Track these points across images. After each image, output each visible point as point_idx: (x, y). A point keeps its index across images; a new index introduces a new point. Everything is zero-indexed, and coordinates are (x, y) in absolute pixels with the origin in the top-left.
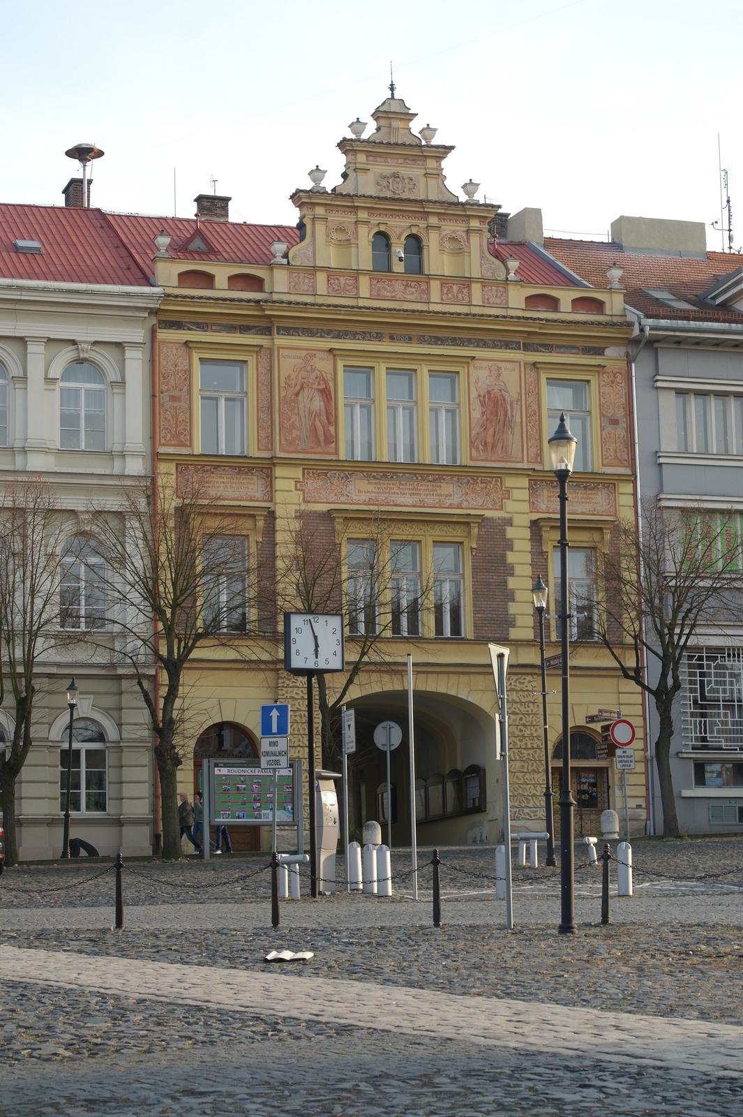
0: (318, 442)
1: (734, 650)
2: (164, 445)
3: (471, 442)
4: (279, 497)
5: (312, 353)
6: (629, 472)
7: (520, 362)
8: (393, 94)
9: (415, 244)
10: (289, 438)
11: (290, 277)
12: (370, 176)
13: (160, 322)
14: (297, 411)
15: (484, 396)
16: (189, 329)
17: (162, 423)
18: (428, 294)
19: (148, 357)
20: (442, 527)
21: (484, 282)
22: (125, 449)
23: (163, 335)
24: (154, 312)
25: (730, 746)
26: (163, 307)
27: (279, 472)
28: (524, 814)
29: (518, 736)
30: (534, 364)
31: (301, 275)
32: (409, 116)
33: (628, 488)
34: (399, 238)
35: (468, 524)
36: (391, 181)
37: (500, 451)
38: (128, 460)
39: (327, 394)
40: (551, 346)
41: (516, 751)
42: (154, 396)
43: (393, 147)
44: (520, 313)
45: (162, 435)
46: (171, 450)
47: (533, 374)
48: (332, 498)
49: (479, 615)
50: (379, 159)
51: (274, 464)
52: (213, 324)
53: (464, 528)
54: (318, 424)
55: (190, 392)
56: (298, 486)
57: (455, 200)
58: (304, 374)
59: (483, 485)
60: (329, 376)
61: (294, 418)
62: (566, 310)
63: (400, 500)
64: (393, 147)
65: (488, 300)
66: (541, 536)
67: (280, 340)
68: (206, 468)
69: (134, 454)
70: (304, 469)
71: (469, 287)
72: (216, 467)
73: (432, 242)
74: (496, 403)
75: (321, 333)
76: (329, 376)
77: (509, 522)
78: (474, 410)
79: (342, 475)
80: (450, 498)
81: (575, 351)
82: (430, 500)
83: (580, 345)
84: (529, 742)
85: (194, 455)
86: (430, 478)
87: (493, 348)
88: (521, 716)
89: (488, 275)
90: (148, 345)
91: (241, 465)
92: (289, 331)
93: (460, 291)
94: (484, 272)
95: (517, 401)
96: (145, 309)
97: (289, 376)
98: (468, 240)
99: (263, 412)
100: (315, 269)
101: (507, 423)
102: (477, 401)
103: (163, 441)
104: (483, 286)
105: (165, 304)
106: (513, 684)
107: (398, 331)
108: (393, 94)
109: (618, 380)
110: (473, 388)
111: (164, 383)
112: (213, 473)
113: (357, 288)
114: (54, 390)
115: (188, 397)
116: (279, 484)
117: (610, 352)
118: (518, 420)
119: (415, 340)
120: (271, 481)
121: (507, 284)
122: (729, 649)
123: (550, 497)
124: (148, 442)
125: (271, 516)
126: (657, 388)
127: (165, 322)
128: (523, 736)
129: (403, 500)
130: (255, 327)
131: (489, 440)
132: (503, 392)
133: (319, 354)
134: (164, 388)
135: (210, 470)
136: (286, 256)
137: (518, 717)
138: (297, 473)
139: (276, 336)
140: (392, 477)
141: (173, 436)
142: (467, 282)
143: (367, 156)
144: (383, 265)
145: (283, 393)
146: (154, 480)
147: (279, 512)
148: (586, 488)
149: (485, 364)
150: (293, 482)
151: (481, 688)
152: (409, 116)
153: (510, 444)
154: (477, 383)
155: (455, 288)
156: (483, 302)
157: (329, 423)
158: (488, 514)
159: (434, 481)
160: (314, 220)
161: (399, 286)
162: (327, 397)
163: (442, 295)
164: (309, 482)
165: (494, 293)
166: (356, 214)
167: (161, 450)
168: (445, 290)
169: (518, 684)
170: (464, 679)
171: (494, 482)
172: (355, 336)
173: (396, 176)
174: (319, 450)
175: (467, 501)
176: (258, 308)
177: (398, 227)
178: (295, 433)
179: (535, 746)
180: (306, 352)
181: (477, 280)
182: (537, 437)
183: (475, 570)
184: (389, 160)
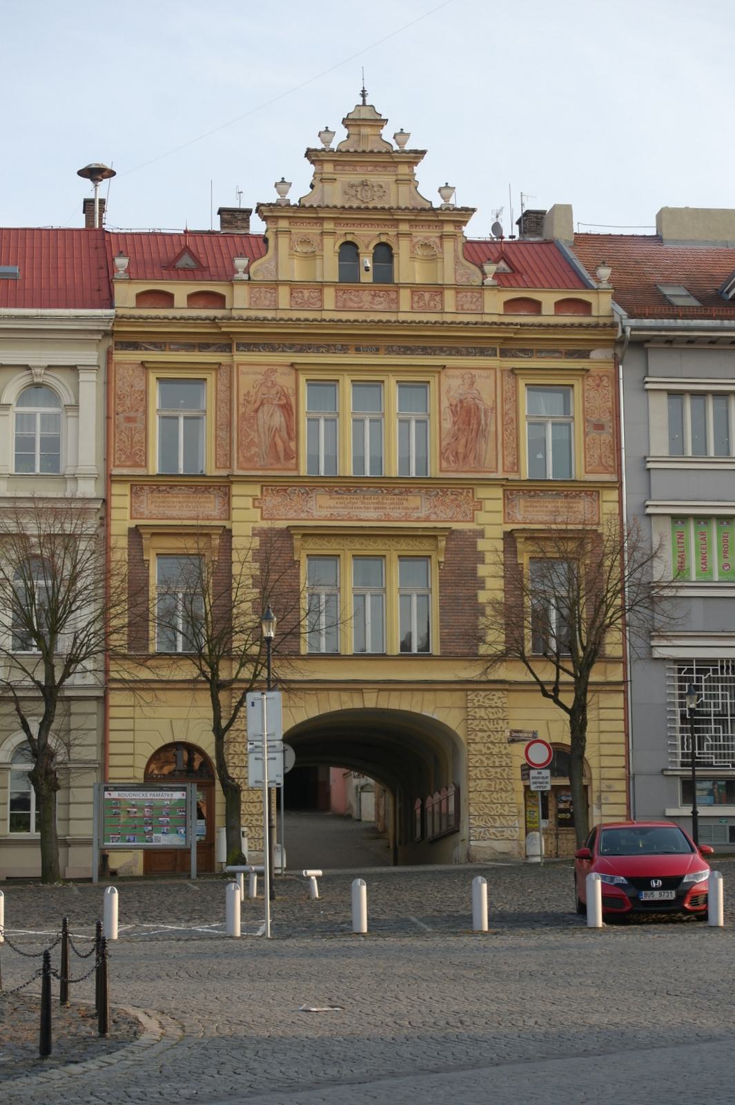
0: (278, 458)
2: (118, 466)
3: (441, 453)
4: (235, 515)
5: (272, 368)
6: (614, 478)
7: (495, 369)
8: (364, 101)
9: (384, 253)
10: (248, 455)
11: (251, 292)
12: (338, 185)
13: (116, 343)
14: (255, 428)
15: (456, 406)
16: (146, 349)
17: (117, 445)
18: (398, 303)
19: (102, 378)
20: (408, 541)
21: (458, 288)
22: (77, 472)
23: (119, 356)
24: (107, 334)
25: (720, 762)
26: (115, 329)
27: (235, 489)
28: (490, 834)
29: (486, 754)
30: (512, 370)
31: (263, 290)
32: (380, 122)
33: (614, 495)
34: (367, 247)
35: (435, 537)
36: (359, 189)
37: (472, 462)
38: (81, 482)
39: (288, 409)
40: (532, 351)
41: (483, 769)
42: (108, 418)
43: (365, 153)
44: (496, 319)
45: (116, 456)
46: (125, 471)
47: (511, 380)
48: (292, 514)
49: (447, 631)
50: (347, 168)
51: (232, 482)
52: (171, 343)
53: (432, 541)
54: (278, 440)
56: (257, 504)
57: (428, 206)
58: (264, 389)
59: (453, 497)
60: (290, 391)
61: (253, 435)
62: (549, 314)
63: (364, 514)
64: (365, 153)
65: (462, 306)
66: (516, 547)
67: (240, 357)
68: (161, 488)
69: (86, 477)
70: (262, 486)
71: (442, 293)
72: (172, 487)
73: (402, 250)
74: (468, 412)
75: (283, 348)
76: (290, 391)
77: (481, 534)
78: (445, 420)
79: (302, 491)
80: (418, 511)
81: (557, 355)
82: (395, 514)
83: (563, 348)
84: (497, 760)
85: (148, 476)
86: (397, 491)
87: (467, 355)
88: (490, 733)
89: (463, 281)
90: (103, 366)
91: (198, 484)
92: (249, 347)
93: (432, 298)
94: (458, 278)
96: (98, 331)
97: (248, 393)
98: (442, 246)
100: (277, 284)
101: (480, 432)
102: (448, 411)
103: (117, 463)
104: (457, 293)
105: (118, 326)
106: (481, 700)
107: (365, 343)
108: (364, 101)
109: (605, 383)
110: (444, 398)
111: (119, 404)
112: (168, 493)
113: (321, 300)
114: (7, 415)
115: (144, 417)
116: (235, 502)
117: (596, 354)
118: (492, 428)
120: (229, 499)
121: (483, 289)
123: (527, 507)
124: (102, 465)
125: (227, 534)
127: (122, 343)
128: (491, 753)
129: (367, 514)
130: (214, 344)
131: (461, 450)
132: (477, 401)
133: (280, 369)
134: (120, 409)
135: (165, 490)
136: (247, 271)
137: (485, 735)
138: (256, 490)
139: (235, 352)
140: (355, 491)
141: (128, 457)
142: (439, 289)
143: (335, 166)
144: (349, 275)
145: (242, 410)
146: (105, 502)
147: (236, 529)
148: (566, 496)
149: (457, 372)
150: (250, 500)
151: (447, 705)
152: (380, 122)
153: (484, 453)
154: (448, 392)
155: (427, 296)
156: (457, 309)
157: (290, 438)
158: (455, 526)
159: (401, 494)
160: (277, 233)
161: (366, 296)
162: (288, 413)
163: (412, 303)
164: (268, 499)
167: (115, 471)
168: (416, 299)
169: (487, 701)
170: (429, 696)
171: (465, 494)
172: (318, 349)
173: (364, 184)
174: (279, 466)
175: (435, 513)
176: (214, 325)
177: (367, 237)
178: (254, 450)
179: (504, 764)
180: (267, 368)
181: (450, 287)
182: (515, 445)
183: (443, 584)
184: (358, 168)
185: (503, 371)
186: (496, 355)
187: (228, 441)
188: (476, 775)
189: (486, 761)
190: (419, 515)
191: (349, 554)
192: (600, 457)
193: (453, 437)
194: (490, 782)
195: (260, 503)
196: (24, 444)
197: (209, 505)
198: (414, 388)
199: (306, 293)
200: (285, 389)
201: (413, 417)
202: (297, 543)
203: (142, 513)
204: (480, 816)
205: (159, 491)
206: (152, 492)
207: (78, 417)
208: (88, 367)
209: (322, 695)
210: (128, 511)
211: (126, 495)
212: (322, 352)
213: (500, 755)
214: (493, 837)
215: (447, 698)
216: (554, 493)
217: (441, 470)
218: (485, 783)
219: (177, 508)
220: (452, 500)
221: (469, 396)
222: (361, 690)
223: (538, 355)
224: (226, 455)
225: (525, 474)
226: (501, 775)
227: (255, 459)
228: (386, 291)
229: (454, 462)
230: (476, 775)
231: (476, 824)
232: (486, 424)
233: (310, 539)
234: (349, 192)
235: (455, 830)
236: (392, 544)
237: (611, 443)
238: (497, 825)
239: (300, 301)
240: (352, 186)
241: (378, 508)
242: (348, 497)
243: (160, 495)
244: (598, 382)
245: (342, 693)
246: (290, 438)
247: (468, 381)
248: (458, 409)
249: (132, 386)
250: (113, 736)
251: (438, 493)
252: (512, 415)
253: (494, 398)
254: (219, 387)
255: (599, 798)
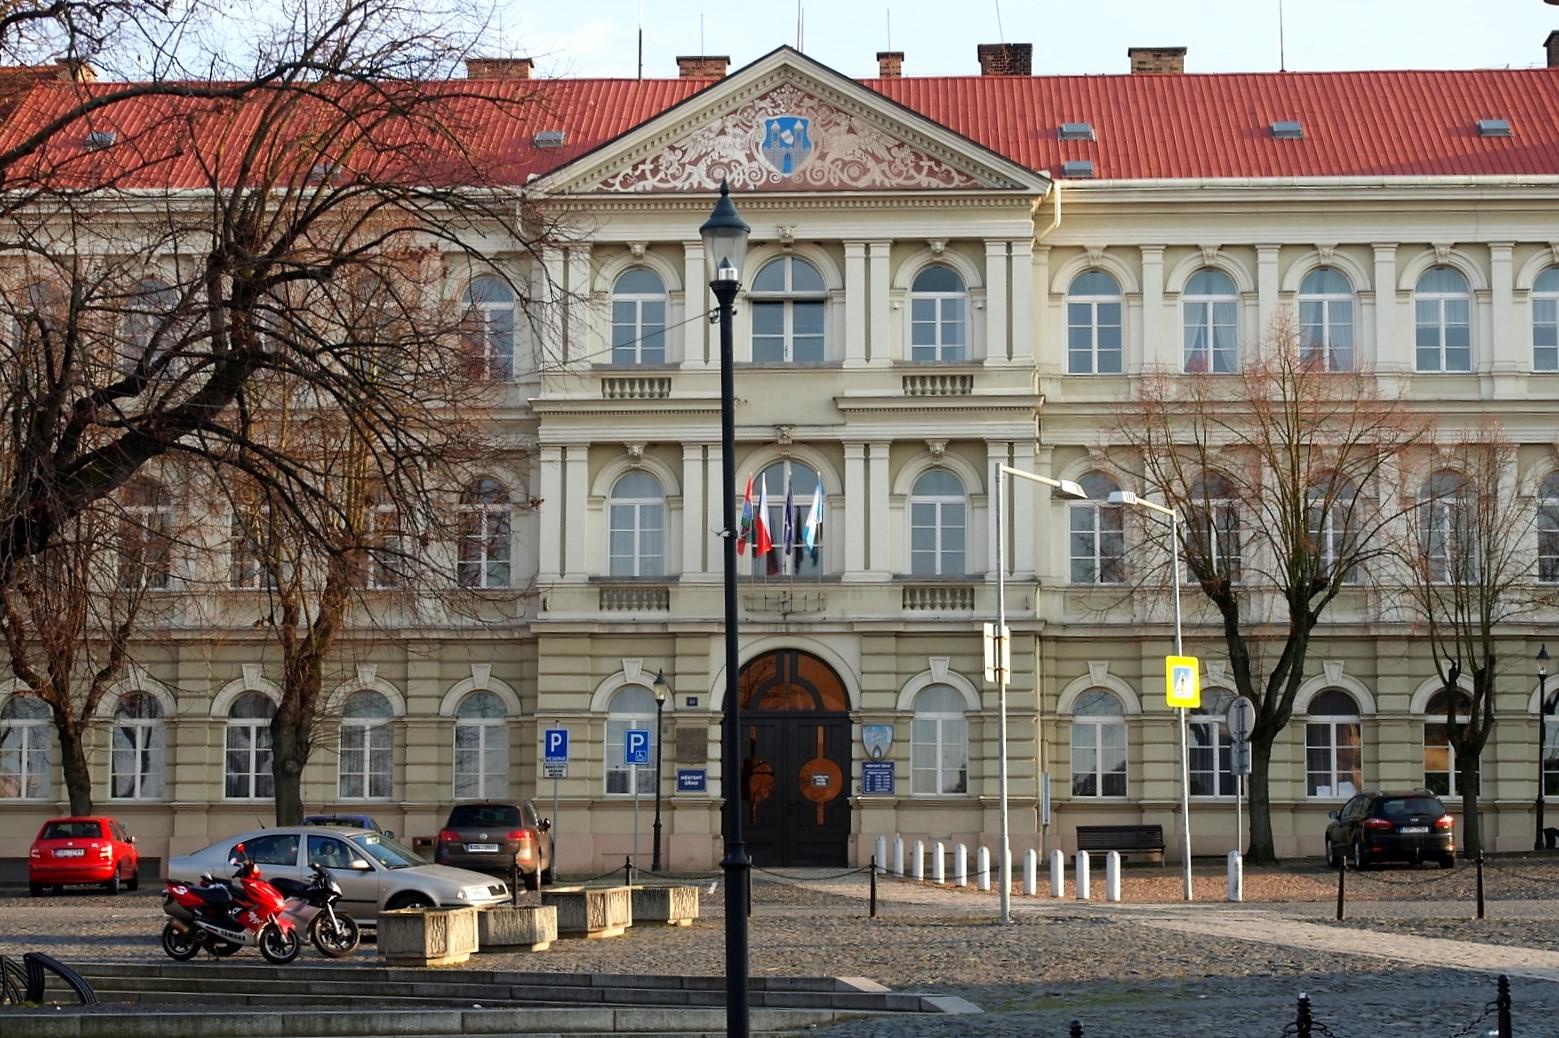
196: (1426, 336)
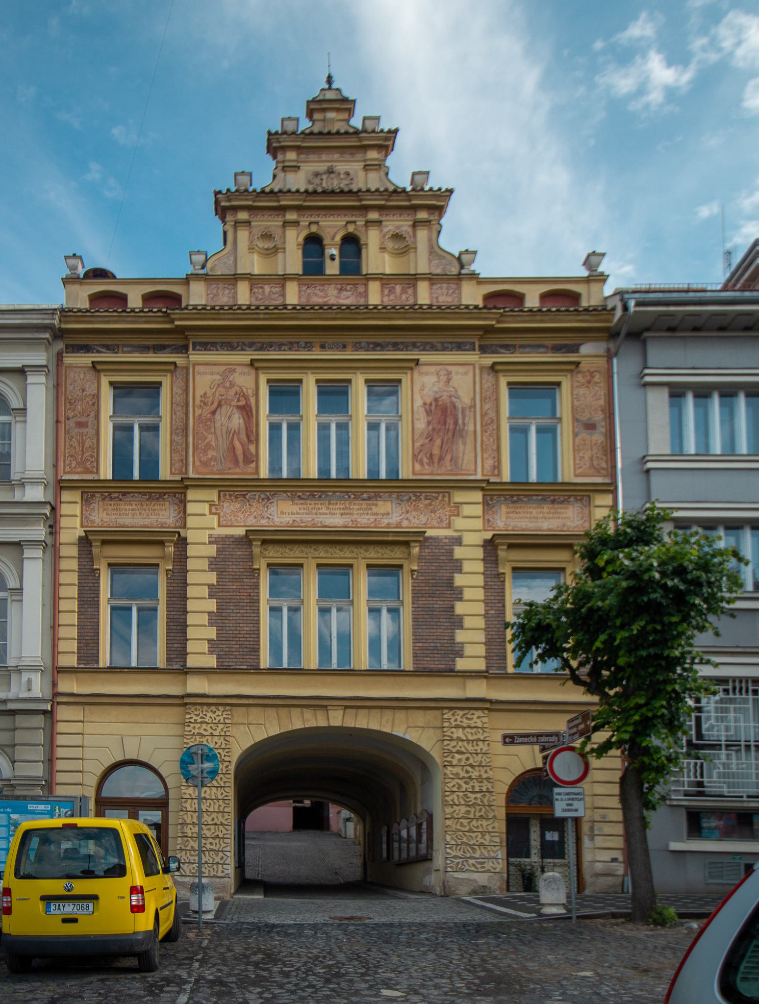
1: (741, 682)
2: (69, 473)
3: (414, 456)
4: (191, 522)
5: (230, 368)
7: (474, 365)
9: (352, 244)
10: (204, 459)
13: (67, 347)
14: (212, 430)
16: (98, 352)
17: (67, 451)
23: (70, 359)
27: (191, 495)
33: (608, 500)
34: (333, 238)
36: (324, 177)
37: (448, 464)
38: (28, 488)
39: (248, 411)
40: (514, 346)
41: (461, 794)
42: (57, 421)
45: (67, 462)
48: (251, 521)
49: (420, 645)
52: (124, 346)
54: (237, 443)
55: (97, 417)
56: (214, 510)
59: (427, 502)
60: (250, 392)
61: (210, 437)
65: (437, 298)
66: (497, 556)
67: (195, 357)
68: (113, 495)
70: (220, 492)
72: (124, 494)
73: (372, 239)
74: (444, 410)
75: (242, 347)
76: (250, 392)
77: (458, 541)
79: (263, 496)
80: (389, 515)
81: (542, 350)
84: (477, 785)
85: (99, 481)
86: (365, 496)
87: (443, 350)
88: (468, 755)
90: (52, 368)
92: (205, 346)
93: (404, 291)
95: (470, 407)
97: (205, 394)
98: (415, 236)
99: (177, 434)
101: (457, 433)
102: (422, 410)
103: (67, 469)
106: (459, 719)
109: (597, 378)
110: (417, 397)
111: (70, 409)
115: (95, 422)
116: (191, 508)
117: (586, 349)
118: (471, 428)
119: (349, 347)
121: (460, 280)
122: (734, 681)
123: (509, 513)
124: (51, 472)
125: (182, 543)
126: (646, 385)
127: (73, 346)
128: (470, 777)
129: (332, 520)
131: (436, 451)
132: (453, 399)
133: (239, 369)
137: (463, 757)
138: (213, 495)
139: (191, 351)
140: (320, 497)
141: (78, 464)
144: (313, 267)
145: (198, 412)
148: (553, 502)
149: (432, 369)
150: (207, 506)
151: (421, 724)
152: (346, 105)
153: (461, 455)
154: (422, 390)
155: (398, 288)
157: (250, 441)
158: (430, 533)
159: (369, 499)
162: (247, 414)
164: (226, 505)
165: (445, 291)
166: (284, 216)
168: (386, 292)
169: (465, 721)
170: (400, 715)
171: (440, 498)
174: (238, 470)
175: (407, 519)
177: (333, 229)
178: (211, 453)
179: (484, 789)
180: (225, 367)
182: (495, 448)
185: (482, 368)
186: (474, 350)
187: (184, 446)
188: (452, 800)
189: (464, 786)
190: (390, 521)
191: (313, 563)
192: (591, 459)
193: (427, 438)
194: (468, 809)
195: (217, 509)
197: (163, 513)
198: (383, 390)
199: (267, 289)
200: (245, 390)
201: (383, 419)
202: (256, 550)
203: (93, 522)
204: (457, 845)
205: (111, 499)
206: (103, 500)
207: (25, 422)
208: (37, 368)
209: (283, 711)
210: (78, 520)
211: (76, 503)
212: (284, 350)
213: (480, 779)
214: (473, 869)
215: (420, 718)
216: (540, 498)
217: (414, 473)
218: (463, 809)
219: (130, 516)
220: (426, 505)
221: (445, 393)
222: (326, 706)
223: (521, 350)
224: (182, 460)
225: (506, 477)
226: (482, 801)
227: (212, 463)
228: (354, 284)
229: (429, 464)
230: (452, 800)
231: (454, 854)
232: (464, 424)
233: (270, 547)
234: (314, 181)
235: (427, 858)
236: (361, 551)
237: (604, 444)
238: (477, 855)
239: (260, 297)
240: (317, 174)
241: (345, 514)
242: (313, 502)
243: (112, 503)
244: (588, 378)
245: (305, 710)
246: (250, 441)
247: (444, 378)
248: (433, 408)
249: (83, 391)
250: (60, 752)
251: (410, 498)
252: (492, 415)
253: (472, 396)
254: (174, 389)
255: (592, 829)
